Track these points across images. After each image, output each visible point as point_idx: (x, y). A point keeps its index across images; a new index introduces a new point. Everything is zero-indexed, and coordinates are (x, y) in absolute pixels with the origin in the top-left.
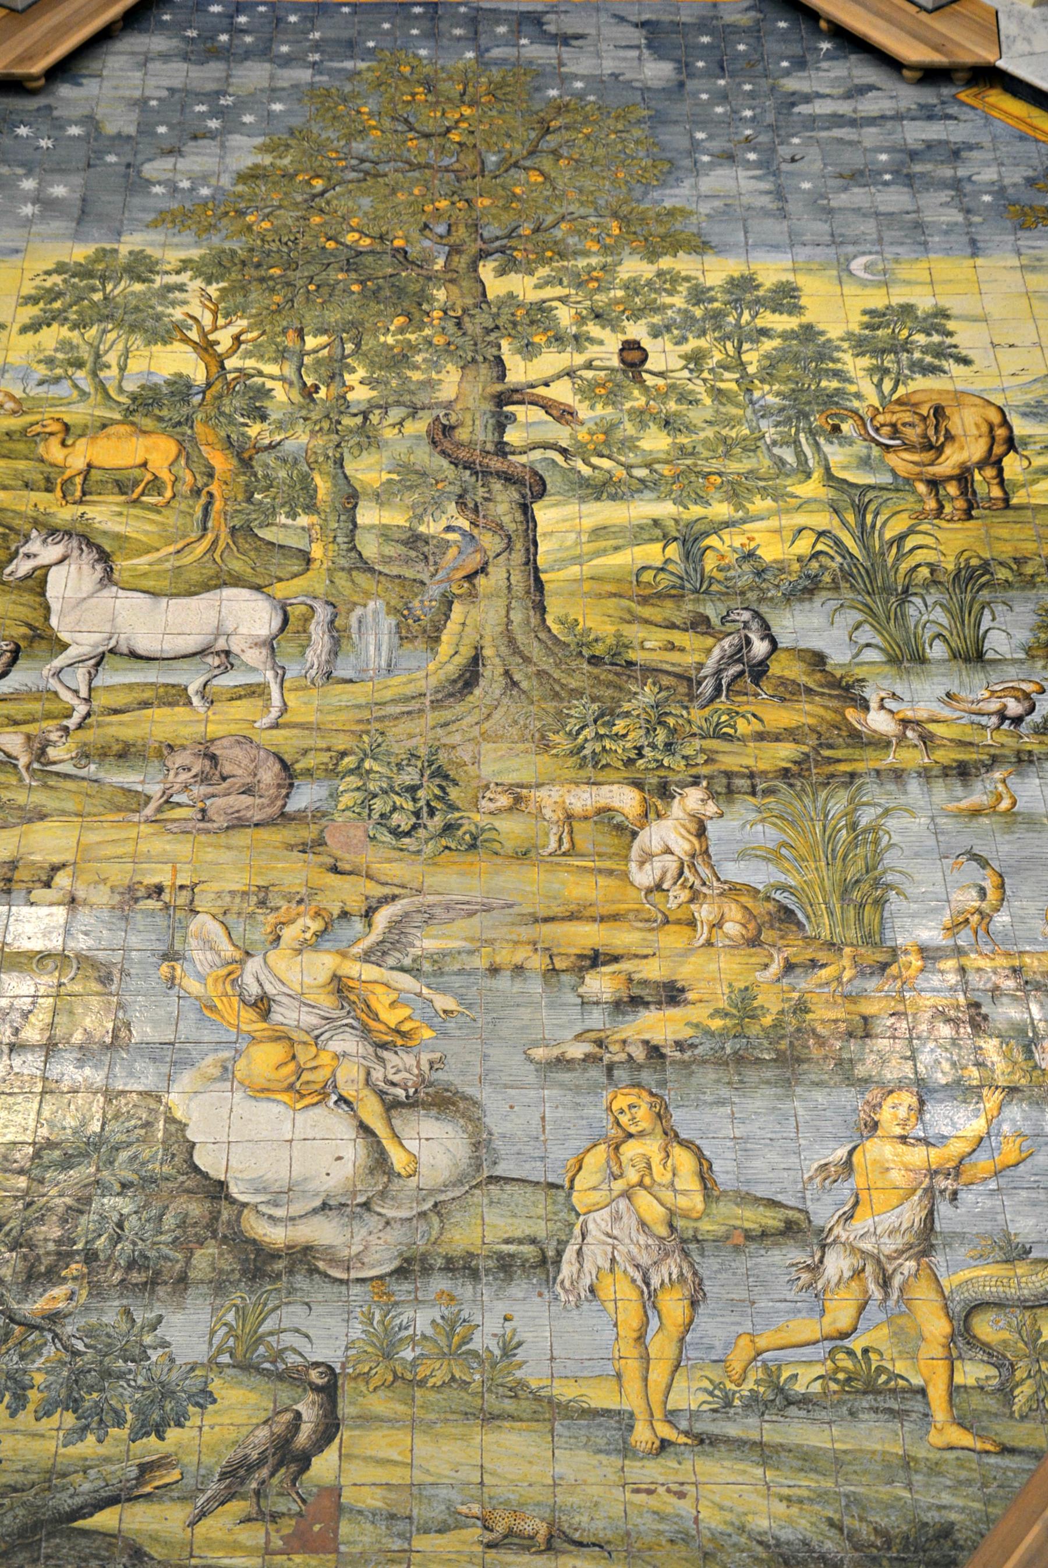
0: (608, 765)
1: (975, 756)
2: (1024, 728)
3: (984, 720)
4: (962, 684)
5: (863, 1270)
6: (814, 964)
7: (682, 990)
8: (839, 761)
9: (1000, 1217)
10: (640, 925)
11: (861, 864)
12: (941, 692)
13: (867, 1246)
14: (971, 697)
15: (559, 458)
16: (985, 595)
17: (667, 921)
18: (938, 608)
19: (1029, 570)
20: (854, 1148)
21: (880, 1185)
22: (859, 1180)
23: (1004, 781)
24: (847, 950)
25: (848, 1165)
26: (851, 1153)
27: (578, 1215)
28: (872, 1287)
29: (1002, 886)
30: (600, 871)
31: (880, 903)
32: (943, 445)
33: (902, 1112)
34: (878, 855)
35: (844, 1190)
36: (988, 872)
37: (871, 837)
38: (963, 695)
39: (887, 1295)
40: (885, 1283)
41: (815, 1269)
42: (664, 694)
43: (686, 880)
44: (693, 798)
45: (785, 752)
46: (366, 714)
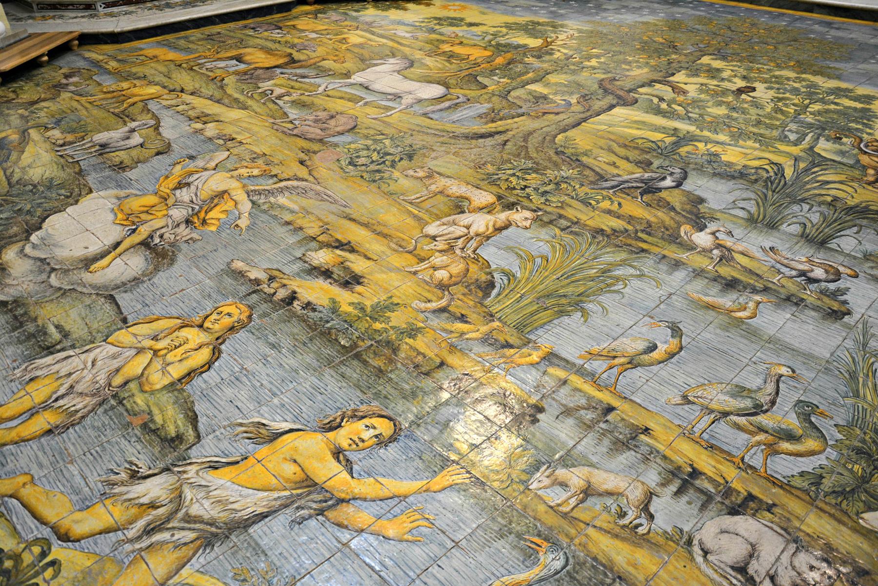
4: (790, 249)
5: (159, 507)
6: (463, 318)
7: (359, 283)
8: (645, 242)
10: (394, 246)
11: (581, 289)
12: (767, 244)
13: (188, 494)
14: (789, 256)
15: (655, 100)
21: (270, 466)
22: (264, 451)
25: (277, 436)
26: (291, 431)
27: (104, 341)
28: (141, 524)
29: (672, 355)
31: (562, 313)
37: (610, 281)
39: (139, 538)
40: (149, 531)
41: (135, 476)
46: (413, 127)
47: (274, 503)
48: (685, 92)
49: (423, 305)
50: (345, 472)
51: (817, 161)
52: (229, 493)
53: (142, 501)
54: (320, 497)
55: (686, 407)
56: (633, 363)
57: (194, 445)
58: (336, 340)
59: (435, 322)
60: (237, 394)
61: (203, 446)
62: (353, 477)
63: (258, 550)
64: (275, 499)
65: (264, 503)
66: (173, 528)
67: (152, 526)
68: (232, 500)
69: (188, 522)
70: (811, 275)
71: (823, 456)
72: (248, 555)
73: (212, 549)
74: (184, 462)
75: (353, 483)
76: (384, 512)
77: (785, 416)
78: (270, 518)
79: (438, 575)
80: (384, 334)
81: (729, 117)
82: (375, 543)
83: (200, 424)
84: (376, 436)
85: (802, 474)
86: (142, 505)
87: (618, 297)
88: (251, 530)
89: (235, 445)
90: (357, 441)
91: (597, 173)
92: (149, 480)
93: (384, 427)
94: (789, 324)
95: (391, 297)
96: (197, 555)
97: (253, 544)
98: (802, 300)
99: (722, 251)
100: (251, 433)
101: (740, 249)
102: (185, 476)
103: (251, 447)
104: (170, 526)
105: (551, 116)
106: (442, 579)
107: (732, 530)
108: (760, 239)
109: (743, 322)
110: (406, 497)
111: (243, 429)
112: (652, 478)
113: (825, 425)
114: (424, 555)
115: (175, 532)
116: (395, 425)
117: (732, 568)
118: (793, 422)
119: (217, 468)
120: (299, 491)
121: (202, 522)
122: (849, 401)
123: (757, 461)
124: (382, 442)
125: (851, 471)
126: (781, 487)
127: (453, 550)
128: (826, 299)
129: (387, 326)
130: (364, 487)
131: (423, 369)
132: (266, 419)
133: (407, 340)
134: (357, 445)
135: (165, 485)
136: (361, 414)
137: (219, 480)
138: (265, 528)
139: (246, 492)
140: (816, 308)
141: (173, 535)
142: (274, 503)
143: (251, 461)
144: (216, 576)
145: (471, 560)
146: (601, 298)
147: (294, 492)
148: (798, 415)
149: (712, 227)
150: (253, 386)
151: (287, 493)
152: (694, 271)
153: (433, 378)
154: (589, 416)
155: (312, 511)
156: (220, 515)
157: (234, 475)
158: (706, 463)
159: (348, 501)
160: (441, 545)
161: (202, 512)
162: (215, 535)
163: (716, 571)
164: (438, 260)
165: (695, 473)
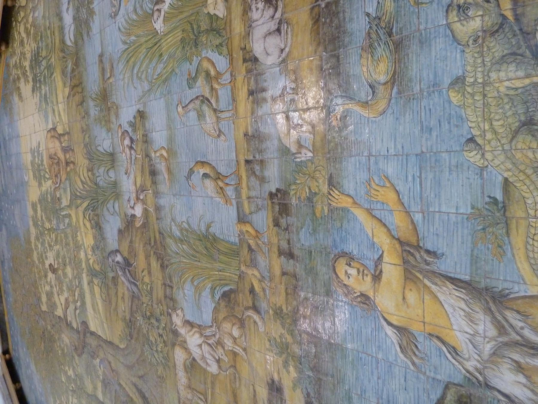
0: (167, 354)
1: (147, 165)
2: (134, 138)
3: (133, 158)
5: (516, 362)
6: (252, 291)
7: (273, 381)
9: (453, 218)
10: (238, 383)
11: (198, 243)
12: (125, 177)
13: (488, 348)
14: (126, 162)
15: (78, 311)
16: (93, 147)
17: (234, 367)
18: (99, 170)
19: (85, 127)
20: (386, 320)
21: (420, 312)
22: (416, 328)
23: (155, 152)
24: (243, 268)
25: (401, 330)
26: (390, 324)
29: (203, 163)
30: (213, 388)
31: (215, 239)
32: (58, 157)
33: (353, 272)
34: (193, 232)
35: (426, 345)
36: (195, 169)
37: (185, 233)
38: (125, 166)
42: (139, 311)
43: (213, 344)
44: (177, 320)
45: (155, 264)
47: (439, 283)
48: (66, 299)
49: (260, 323)
50: (384, 261)
51: (74, 197)
52: (460, 319)
53: (523, 380)
54: (411, 258)
55: (223, 130)
56: (218, 177)
57: (455, 384)
58: (315, 356)
59: (263, 305)
60: (398, 390)
61: (450, 376)
62: (383, 252)
63: (474, 260)
64: (436, 284)
65: (445, 289)
66: (518, 334)
67: (532, 351)
68: (462, 313)
69: (503, 327)
70: (129, 144)
71: (208, 55)
72: (483, 263)
73: (503, 290)
74: (471, 377)
75: (386, 248)
76: (386, 212)
77: (201, 87)
78: (449, 275)
79: (393, 146)
80: (291, 328)
81: (70, 262)
82: (406, 198)
83: (438, 396)
84: (350, 265)
85: (220, 54)
86: (526, 377)
87: (190, 220)
88: (467, 278)
89: (429, 352)
90: (361, 274)
91: (132, 301)
92: (506, 391)
93: (342, 267)
94: (158, 129)
95: (267, 349)
96: (517, 295)
97: (474, 268)
98: (143, 135)
99: (140, 195)
100: (412, 350)
101: (134, 187)
102: (479, 366)
103: (421, 339)
104: (518, 338)
105: (113, 365)
106: (393, 142)
107: (265, 52)
108: (124, 183)
109: (168, 149)
110: (367, 210)
111: (414, 358)
112: (265, 108)
113: (193, 68)
114: (389, 165)
115: (518, 329)
116: (335, 262)
117: (280, 34)
118: (201, 81)
119: (454, 348)
120: (418, 275)
121: (494, 317)
122: (177, 71)
123: (227, 77)
124: (350, 259)
125: (206, 40)
126: (232, 55)
127: (374, 154)
128: (137, 127)
129: (286, 333)
130: (383, 240)
131: (294, 282)
132: (396, 350)
133: (285, 310)
134: (364, 270)
135: (499, 374)
136: (345, 289)
137: (459, 337)
138: (458, 270)
139: (449, 310)
140: (144, 126)
141: (522, 328)
142: (439, 283)
143: (428, 329)
144: (515, 267)
145: (371, 140)
146: (196, 228)
147: (421, 277)
148: (195, 83)
149: (130, 212)
150: (384, 384)
151: (426, 282)
152: (156, 197)
153: (294, 270)
154: (257, 168)
155: (422, 254)
156: (478, 310)
157: (448, 331)
158: (243, 94)
159: (398, 239)
160: (376, 163)
161: (489, 325)
162: (493, 298)
163: (287, 39)
164: (229, 343)
165: (251, 93)
